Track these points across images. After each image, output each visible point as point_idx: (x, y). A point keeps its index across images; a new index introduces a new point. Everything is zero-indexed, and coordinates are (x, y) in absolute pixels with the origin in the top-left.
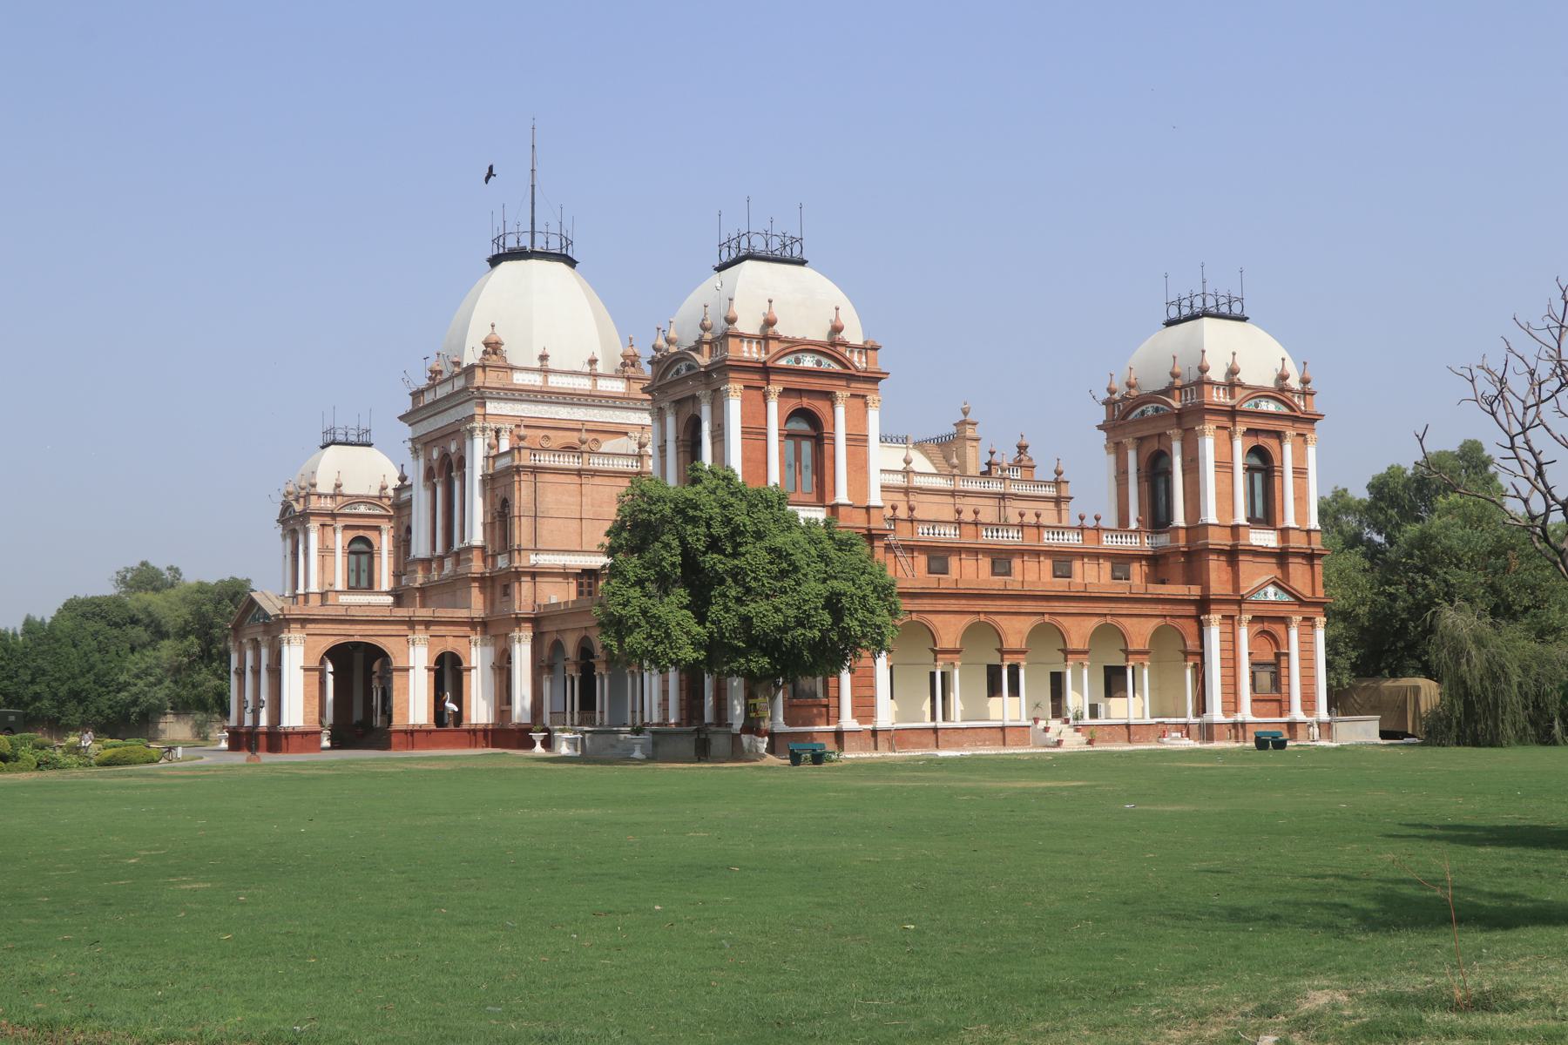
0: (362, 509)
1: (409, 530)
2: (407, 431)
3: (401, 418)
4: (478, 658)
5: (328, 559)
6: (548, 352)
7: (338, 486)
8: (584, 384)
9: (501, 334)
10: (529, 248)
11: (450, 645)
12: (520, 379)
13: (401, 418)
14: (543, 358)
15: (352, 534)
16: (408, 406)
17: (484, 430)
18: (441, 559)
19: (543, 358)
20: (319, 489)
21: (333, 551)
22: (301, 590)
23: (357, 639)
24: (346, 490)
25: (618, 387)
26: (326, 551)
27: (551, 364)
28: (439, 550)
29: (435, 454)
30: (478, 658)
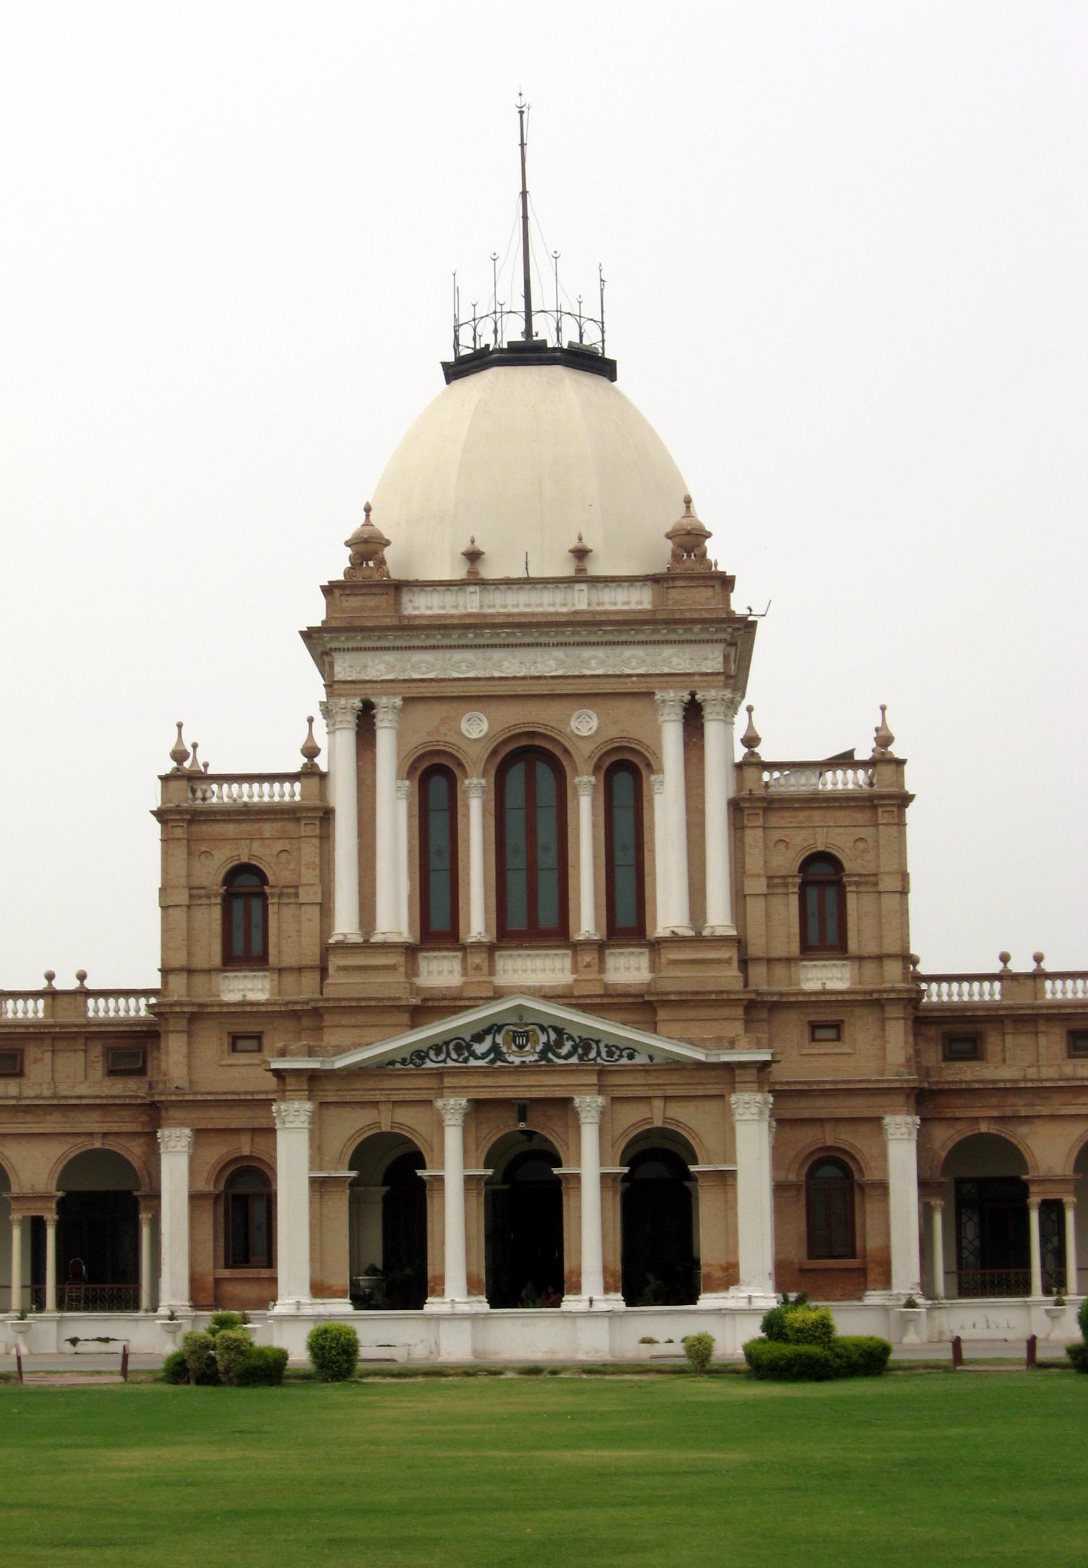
18: (491, 949)
28: (477, 922)
29: (476, 728)
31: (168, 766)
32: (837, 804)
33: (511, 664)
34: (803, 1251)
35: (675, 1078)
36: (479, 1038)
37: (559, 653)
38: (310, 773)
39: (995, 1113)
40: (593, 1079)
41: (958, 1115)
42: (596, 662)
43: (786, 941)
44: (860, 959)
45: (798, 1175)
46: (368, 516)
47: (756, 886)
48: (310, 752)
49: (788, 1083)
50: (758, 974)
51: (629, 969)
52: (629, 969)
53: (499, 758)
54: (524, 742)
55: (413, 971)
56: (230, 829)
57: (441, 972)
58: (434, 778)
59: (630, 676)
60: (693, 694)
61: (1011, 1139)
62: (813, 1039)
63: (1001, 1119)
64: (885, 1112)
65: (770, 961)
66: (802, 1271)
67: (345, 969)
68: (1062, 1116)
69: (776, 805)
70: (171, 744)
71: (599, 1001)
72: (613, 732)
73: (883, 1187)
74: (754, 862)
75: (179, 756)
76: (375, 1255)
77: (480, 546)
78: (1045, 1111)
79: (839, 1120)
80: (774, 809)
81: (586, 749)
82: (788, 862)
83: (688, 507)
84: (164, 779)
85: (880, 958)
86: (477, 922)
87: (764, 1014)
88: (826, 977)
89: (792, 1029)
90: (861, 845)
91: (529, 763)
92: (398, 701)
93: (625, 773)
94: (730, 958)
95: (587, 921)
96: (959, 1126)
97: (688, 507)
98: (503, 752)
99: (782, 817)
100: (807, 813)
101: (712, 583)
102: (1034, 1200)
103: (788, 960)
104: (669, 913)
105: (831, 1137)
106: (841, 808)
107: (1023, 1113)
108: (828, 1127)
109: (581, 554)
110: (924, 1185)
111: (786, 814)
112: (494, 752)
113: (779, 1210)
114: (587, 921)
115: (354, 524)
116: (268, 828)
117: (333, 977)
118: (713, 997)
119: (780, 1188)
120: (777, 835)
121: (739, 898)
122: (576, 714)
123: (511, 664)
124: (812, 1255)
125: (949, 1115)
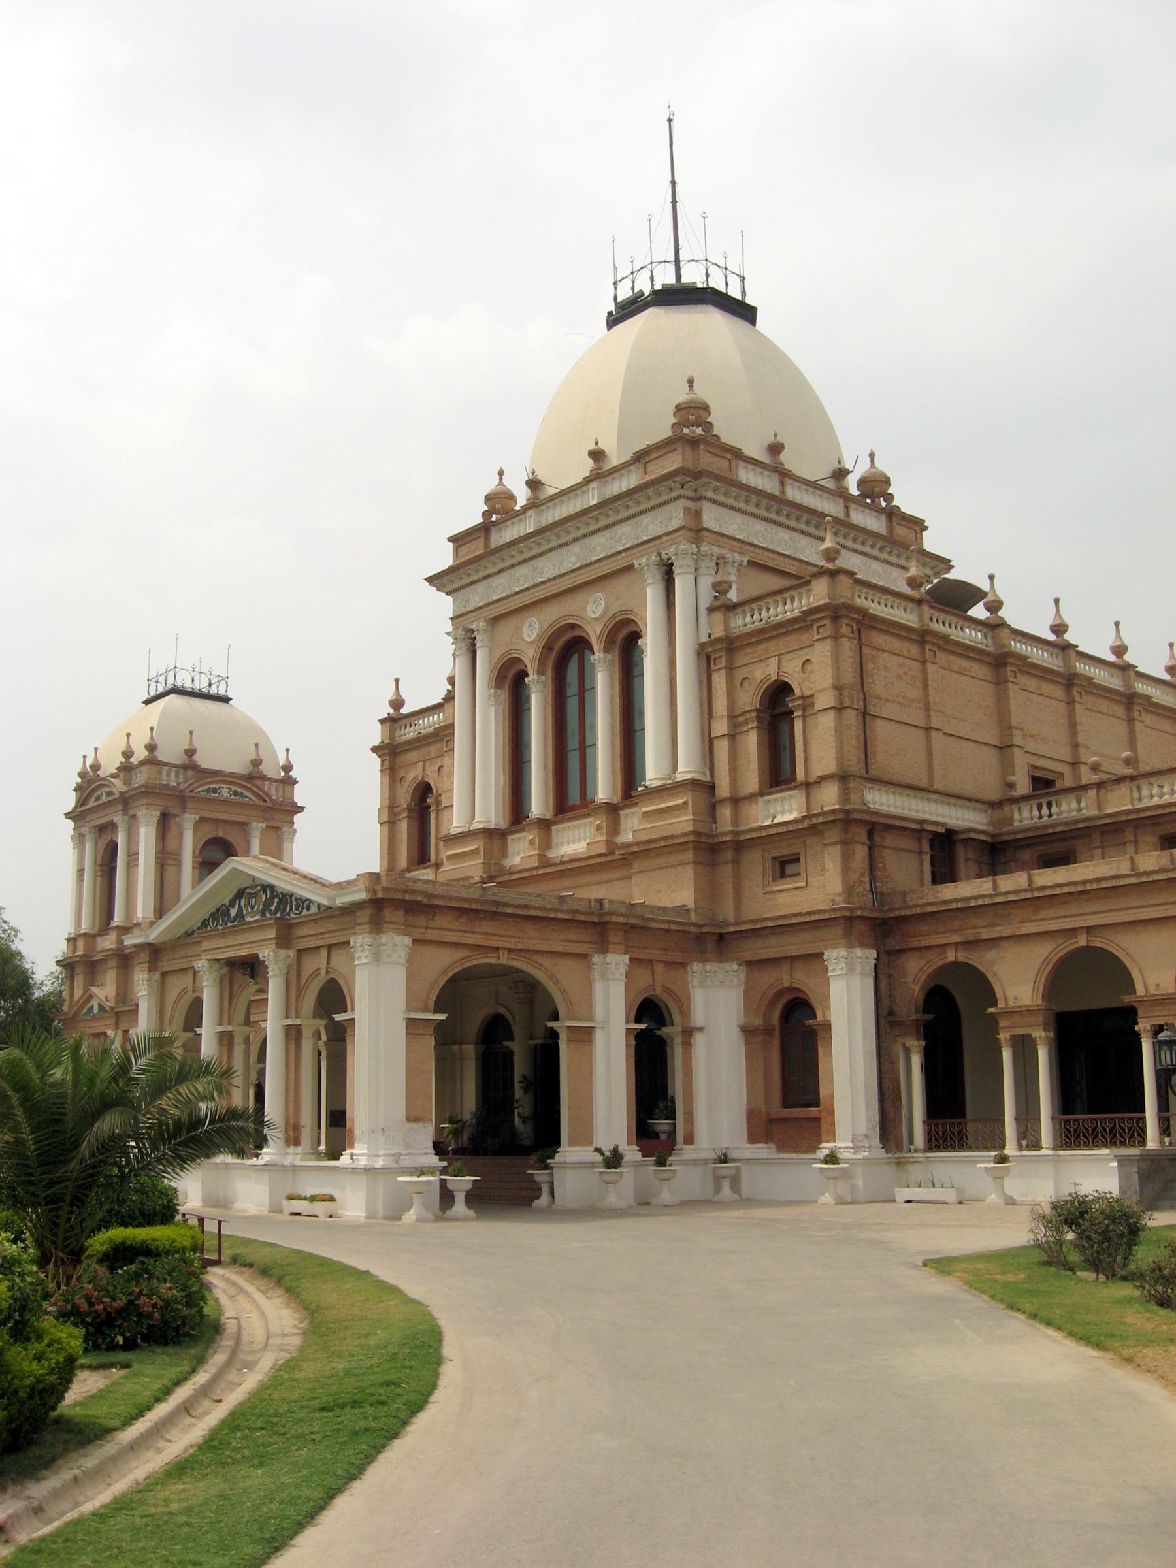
0: (225, 793)
1: (424, 790)
2: (443, 605)
3: (431, 580)
4: (717, 1010)
5: (170, 871)
6: (780, 439)
7: (190, 753)
8: (831, 507)
9: (702, 392)
10: (700, 285)
11: (658, 982)
12: (747, 476)
13: (431, 580)
14: (775, 449)
15: (208, 832)
16: (444, 558)
17: (698, 557)
19: (775, 449)
20: (162, 755)
21: (177, 859)
22: (118, 919)
23: (504, 959)
24: (205, 760)
25: (874, 523)
26: (166, 859)
27: (788, 459)
28: (538, 803)
30: (717, 1010)
31: (387, 711)
32: (784, 630)
33: (548, 568)
34: (777, 1098)
35: (330, 925)
36: (232, 904)
37: (576, 548)
38: (449, 698)
39: (956, 938)
40: (272, 934)
41: (923, 944)
42: (600, 546)
43: (751, 780)
44: (808, 786)
45: (767, 1018)
46: (501, 479)
47: (721, 727)
48: (451, 680)
49: (751, 921)
50: (725, 813)
51: (634, 826)
52: (634, 826)
53: (553, 656)
54: (569, 635)
55: (504, 853)
56: (413, 756)
57: (521, 852)
58: (512, 680)
59: (619, 553)
60: (660, 555)
61: (980, 967)
62: (783, 875)
63: (968, 944)
64: (826, 948)
65: (736, 801)
66: (771, 1120)
67: (450, 857)
68: (1028, 935)
69: (738, 644)
70: (390, 695)
71: (604, 859)
72: (614, 609)
73: (827, 1026)
74: (720, 704)
75: (397, 703)
76: (469, 1103)
77: (540, 476)
78: (1005, 931)
79: (794, 959)
80: (737, 649)
81: (598, 629)
82: (749, 699)
83: (691, 387)
84: (382, 721)
85: (822, 779)
86: (538, 803)
87: (729, 855)
88: (785, 809)
89: (756, 865)
90: (808, 668)
91: (567, 650)
92: (482, 624)
93: (626, 642)
94: (685, 803)
95: (604, 788)
96: (930, 955)
97: (691, 387)
98: (558, 646)
99: (746, 655)
100: (764, 646)
101: (673, 447)
102: (1003, 1036)
103: (752, 797)
104: (653, 772)
105: (784, 978)
106: (788, 633)
107: (984, 936)
108: (786, 966)
109: (597, 455)
110: (886, 1021)
111: (749, 651)
112: (548, 648)
113: (749, 1057)
114: (604, 788)
115: (491, 485)
116: (433, 750)
117: (447, 866)
118: (662, 844)
119: (748, 1032)
120: (741, 674)
121: (708, 743)
122: (591, 600)
123: (548, 568)
124: (786, 1104)
125: (916, 944)
